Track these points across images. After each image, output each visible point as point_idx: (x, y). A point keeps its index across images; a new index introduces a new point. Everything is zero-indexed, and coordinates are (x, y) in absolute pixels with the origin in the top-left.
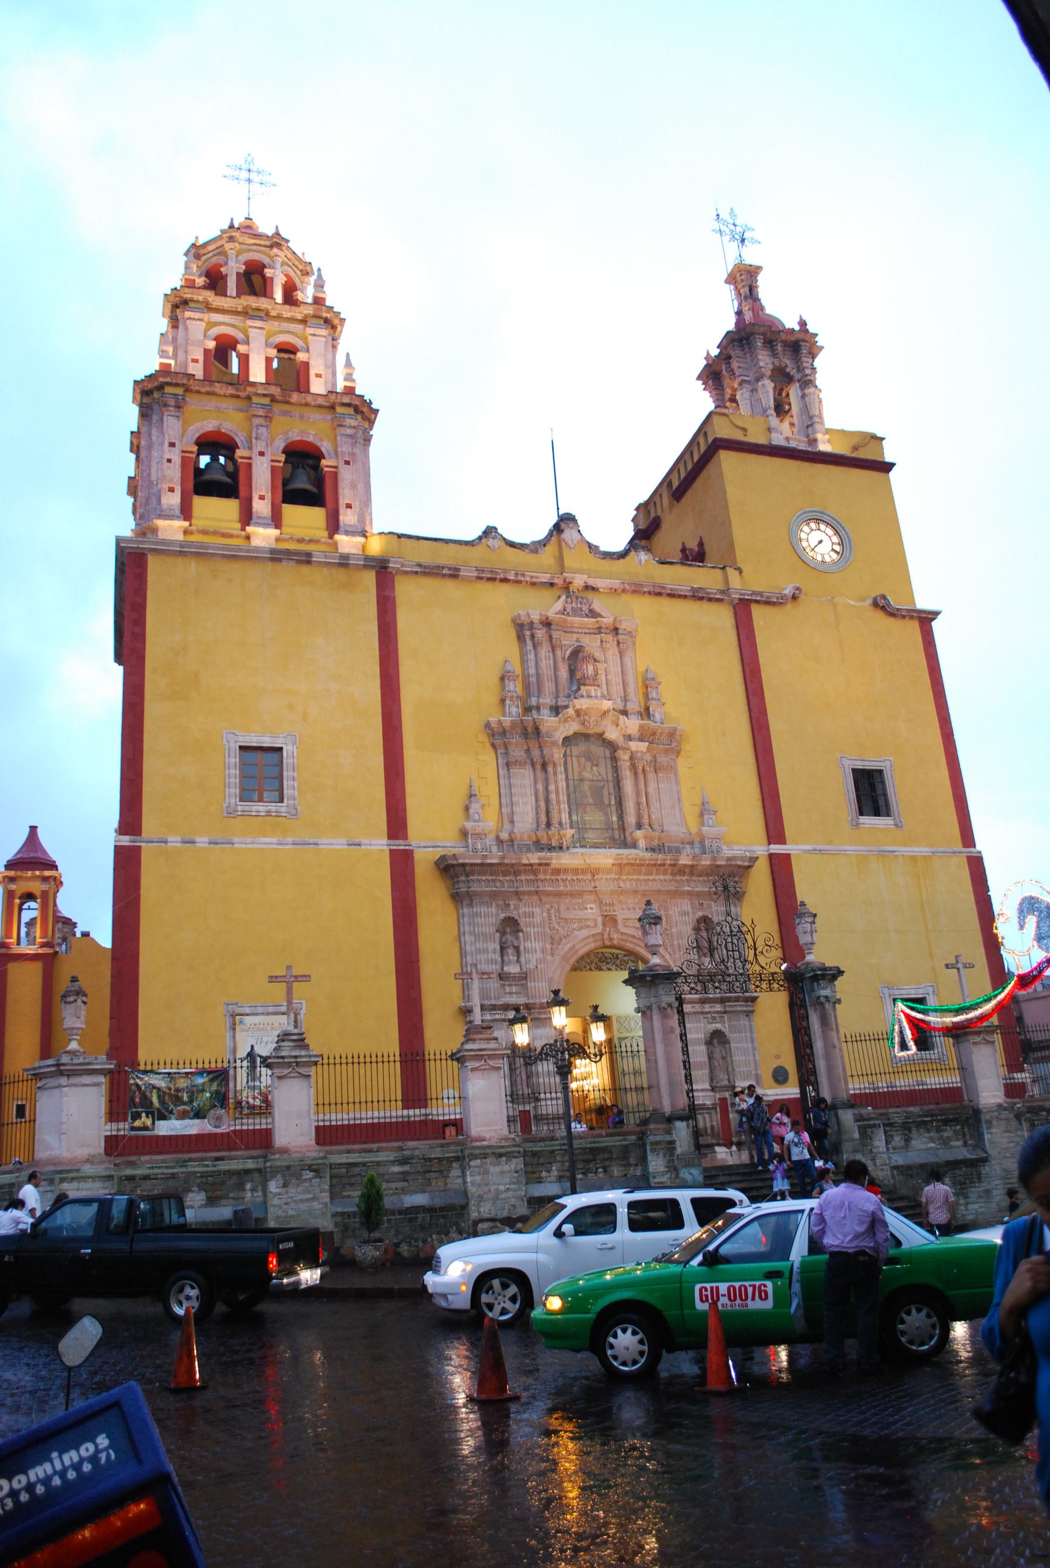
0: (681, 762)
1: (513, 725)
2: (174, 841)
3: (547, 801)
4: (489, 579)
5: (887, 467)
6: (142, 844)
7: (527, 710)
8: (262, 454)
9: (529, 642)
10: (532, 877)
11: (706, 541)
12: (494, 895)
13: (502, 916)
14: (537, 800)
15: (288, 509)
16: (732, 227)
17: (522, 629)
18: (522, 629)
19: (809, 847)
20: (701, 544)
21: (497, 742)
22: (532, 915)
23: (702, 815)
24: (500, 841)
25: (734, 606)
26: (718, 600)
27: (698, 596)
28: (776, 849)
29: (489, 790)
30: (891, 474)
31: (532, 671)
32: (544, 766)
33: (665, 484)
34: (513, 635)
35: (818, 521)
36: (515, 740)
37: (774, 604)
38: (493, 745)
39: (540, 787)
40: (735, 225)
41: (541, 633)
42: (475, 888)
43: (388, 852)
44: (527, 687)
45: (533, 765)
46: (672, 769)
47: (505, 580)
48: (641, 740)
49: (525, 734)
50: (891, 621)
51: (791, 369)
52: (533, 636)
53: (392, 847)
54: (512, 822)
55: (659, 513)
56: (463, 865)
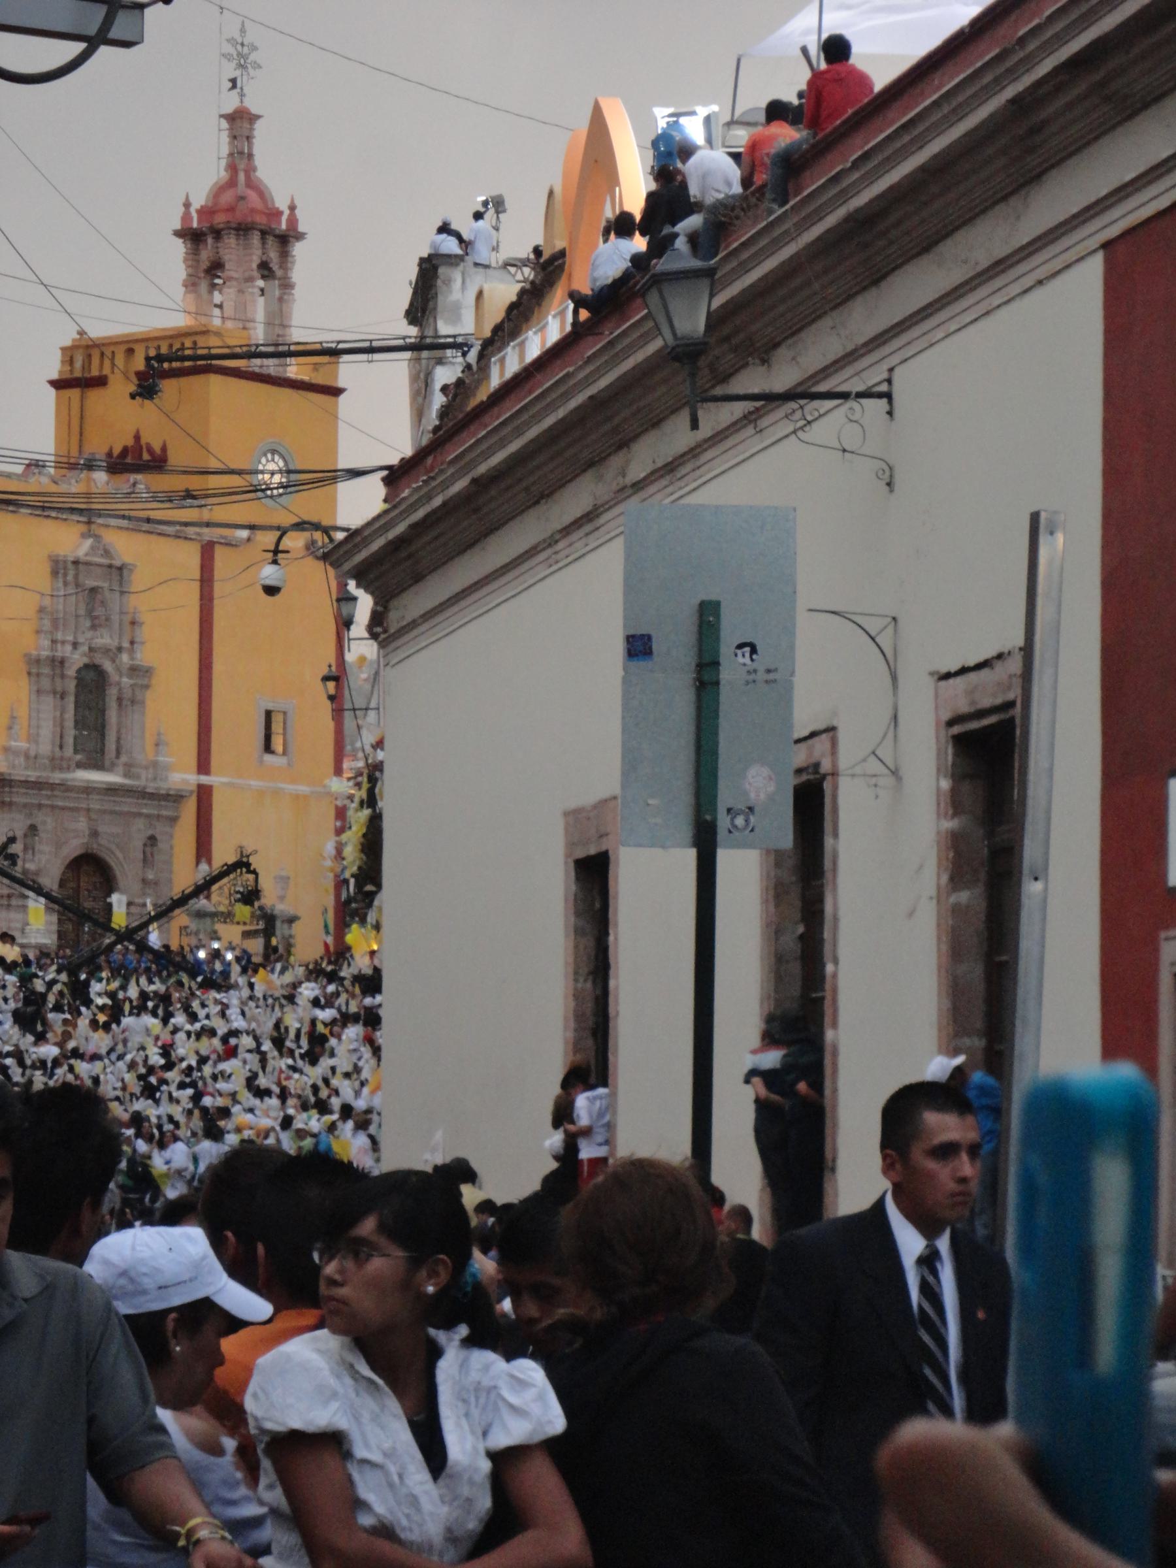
0: (149, 696)
1: (48, 657)
3: (62, 727)
7: (54, 642)
9: (61, 580)
10: (49, 793)
11: (169, 447)
12: (25, 805)
13: (29, 822)
14: (54, 726)
16: (239, 47)
17: (58, 567)
18: (58, 567)
19: (225, 780)
20: (164, 449)
21: (34, 671)
22: (44, 823)
23: (157, 745)
24: (27, 757)
25: (202, 547)
28: (204, 779)
29: (23, 712)
30: (342, 398)
31: (61, 607)
32: (62, 698)
33: (124, 347)
34: (47, 568)
35: (274, 452)
36: (46, 670)
37: (232, 545)
38: (29, 674)
39: (58, 714)
40: (242, 45)
42: (14, 800)
44: (55, 623)
45: (55, 693)
46: (143, 703)
51: (275, 266)
52: (65, 575)
54: (37, 742)
55: (106, 371)
56: (12, 780)
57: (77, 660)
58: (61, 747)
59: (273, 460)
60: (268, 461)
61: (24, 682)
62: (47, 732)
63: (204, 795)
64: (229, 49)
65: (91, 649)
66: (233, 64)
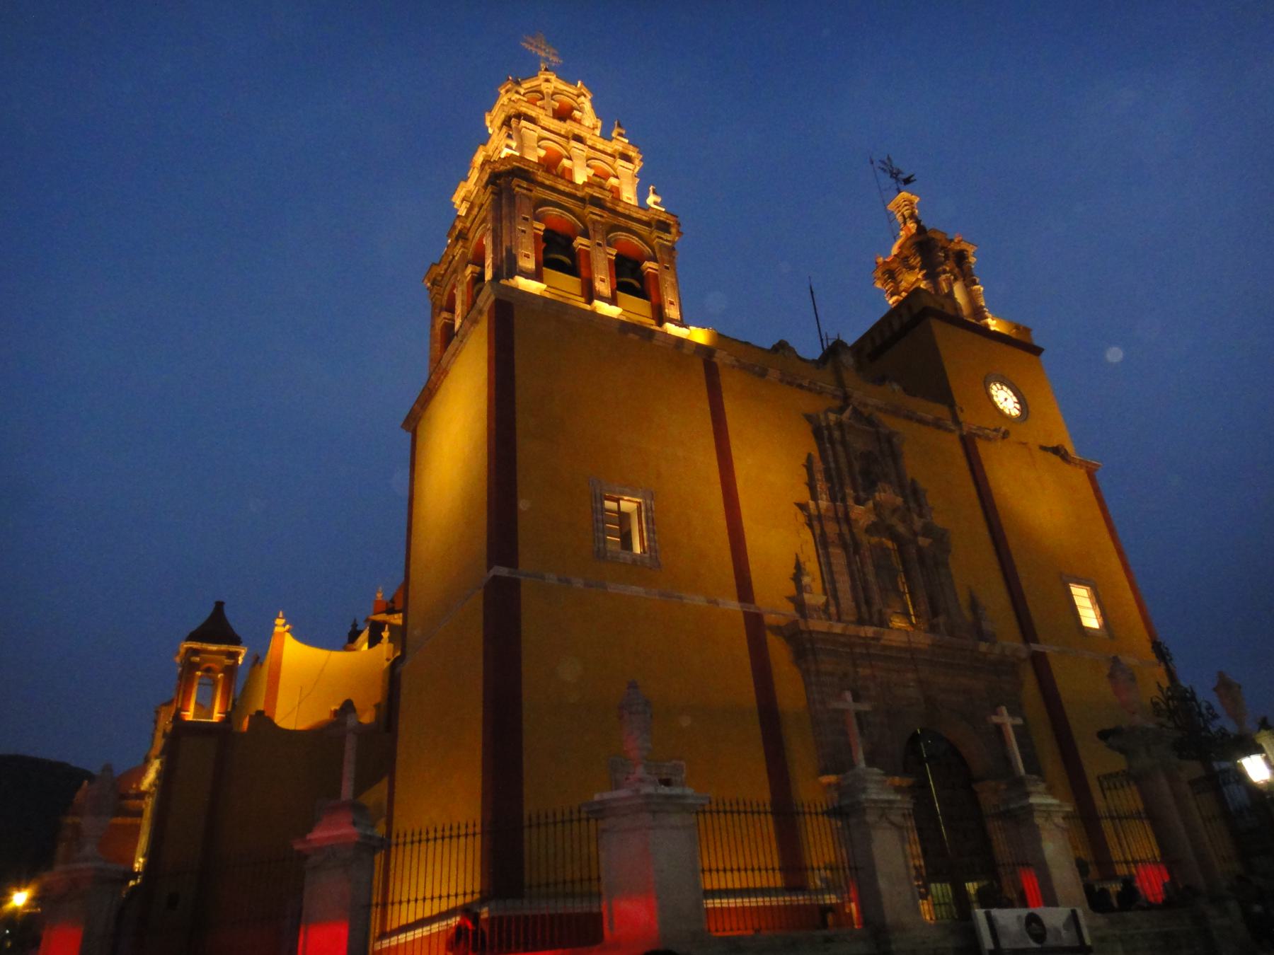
1: (827, 510)
2: (552, 578)
4: (790, 384)
5: (1037, 351)
6: (522, 578)
8: (599, 245)
15: (621, 295)
26: (951, 431)
27: (938, 424)
28: (1034, 647)
29: (812, 566)
31: (832, 465)
32: (856, 552)
38: (811, 526)
41: (837, 434)
43: (741, 615)
45: (845, 547)
47: (800, 386)
48: (925, 535)
49: (837, 520)
50: (1067, 467)
52: (830, 435)
53: (745, 609)
54: (836, 597)
57: (861, 514)
58: (868, 603)
59: (1002, 389)
60: (998, 389)
61: (807, 535)
62: (844, 584)
63: (1040, 663)
64: (882, 166)
65: (875, 505)
66: (889, 175)
